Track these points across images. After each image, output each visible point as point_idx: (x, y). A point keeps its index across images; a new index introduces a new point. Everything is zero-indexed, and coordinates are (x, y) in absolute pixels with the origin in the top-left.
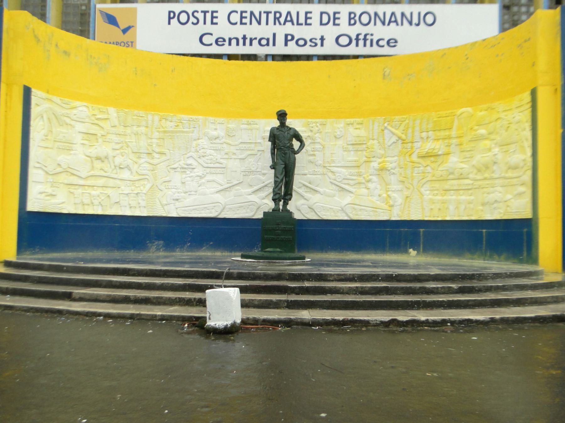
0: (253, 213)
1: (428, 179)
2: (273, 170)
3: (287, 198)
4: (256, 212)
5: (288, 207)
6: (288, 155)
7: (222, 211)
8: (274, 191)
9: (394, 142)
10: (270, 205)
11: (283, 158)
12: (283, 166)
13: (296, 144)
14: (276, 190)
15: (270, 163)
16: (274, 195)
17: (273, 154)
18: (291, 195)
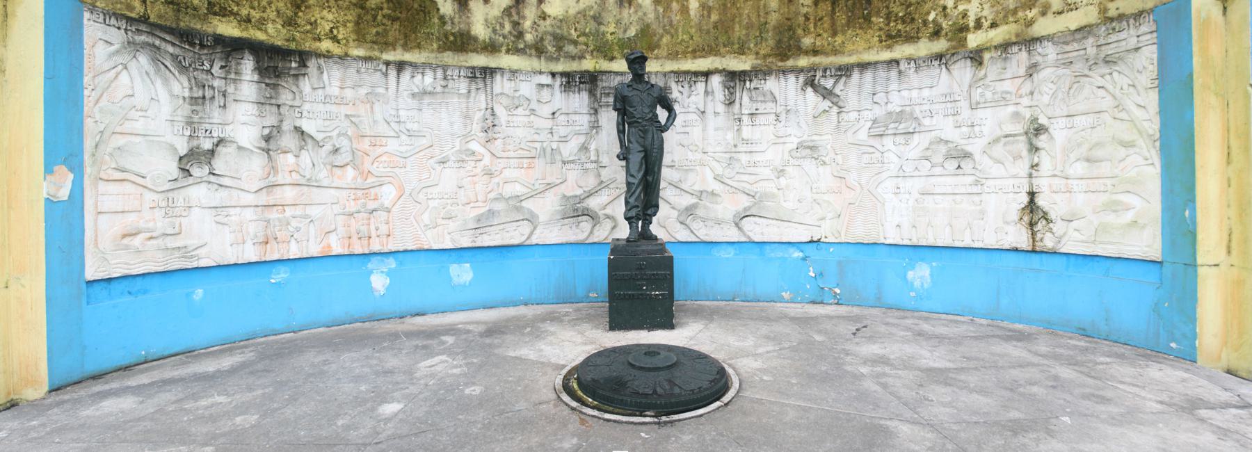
0: (586, 234)
1: (889, 173)
2: (624, 163)
3: (649, 212)
4: (591, 232)
5: (654, 229)
6: (650, 136)
7: (532, 233)
8: (627, 203)
9: (825, 111)
10: (624, 231)
11: (641, 140)
12: (642, 155)
13: (662, 115)
14: (632, 200)
15: (617, 150)
16: (628, 210)
17: (621, 132)
18: (657, 206)
